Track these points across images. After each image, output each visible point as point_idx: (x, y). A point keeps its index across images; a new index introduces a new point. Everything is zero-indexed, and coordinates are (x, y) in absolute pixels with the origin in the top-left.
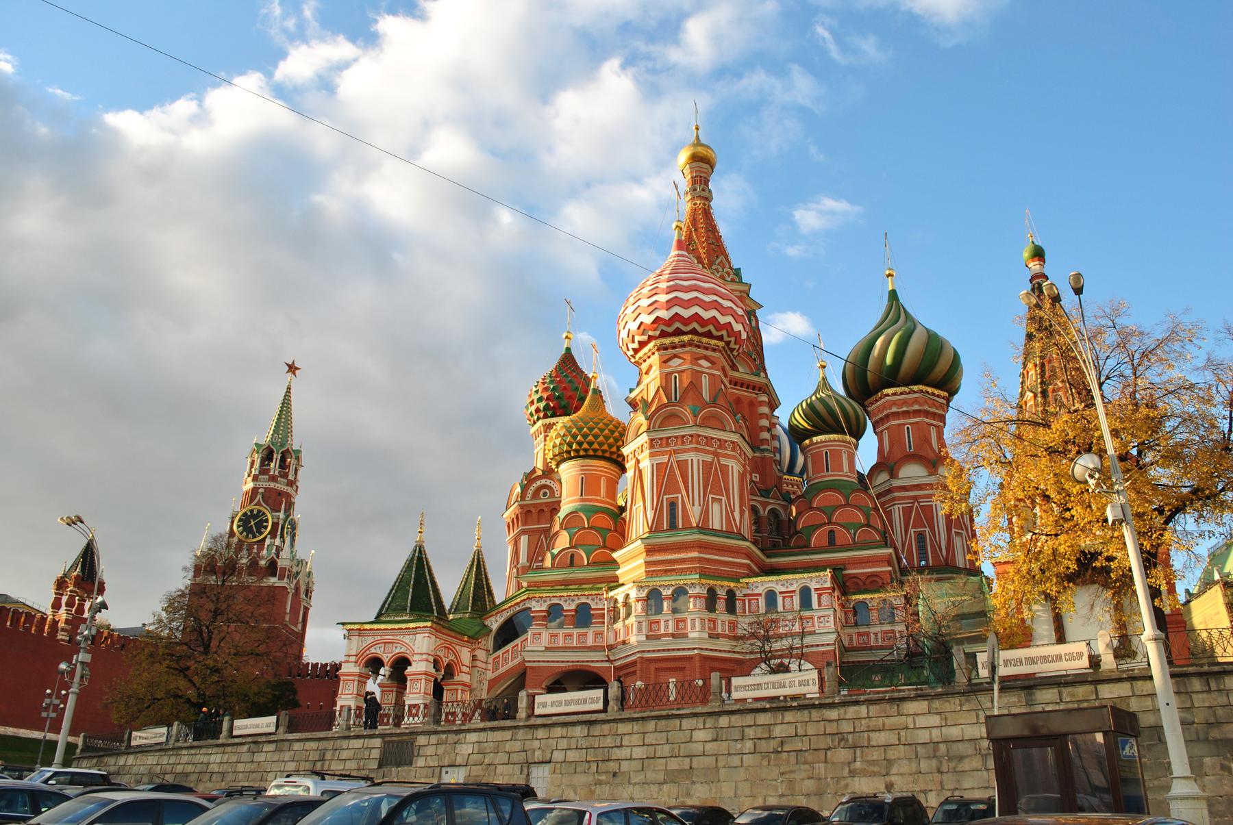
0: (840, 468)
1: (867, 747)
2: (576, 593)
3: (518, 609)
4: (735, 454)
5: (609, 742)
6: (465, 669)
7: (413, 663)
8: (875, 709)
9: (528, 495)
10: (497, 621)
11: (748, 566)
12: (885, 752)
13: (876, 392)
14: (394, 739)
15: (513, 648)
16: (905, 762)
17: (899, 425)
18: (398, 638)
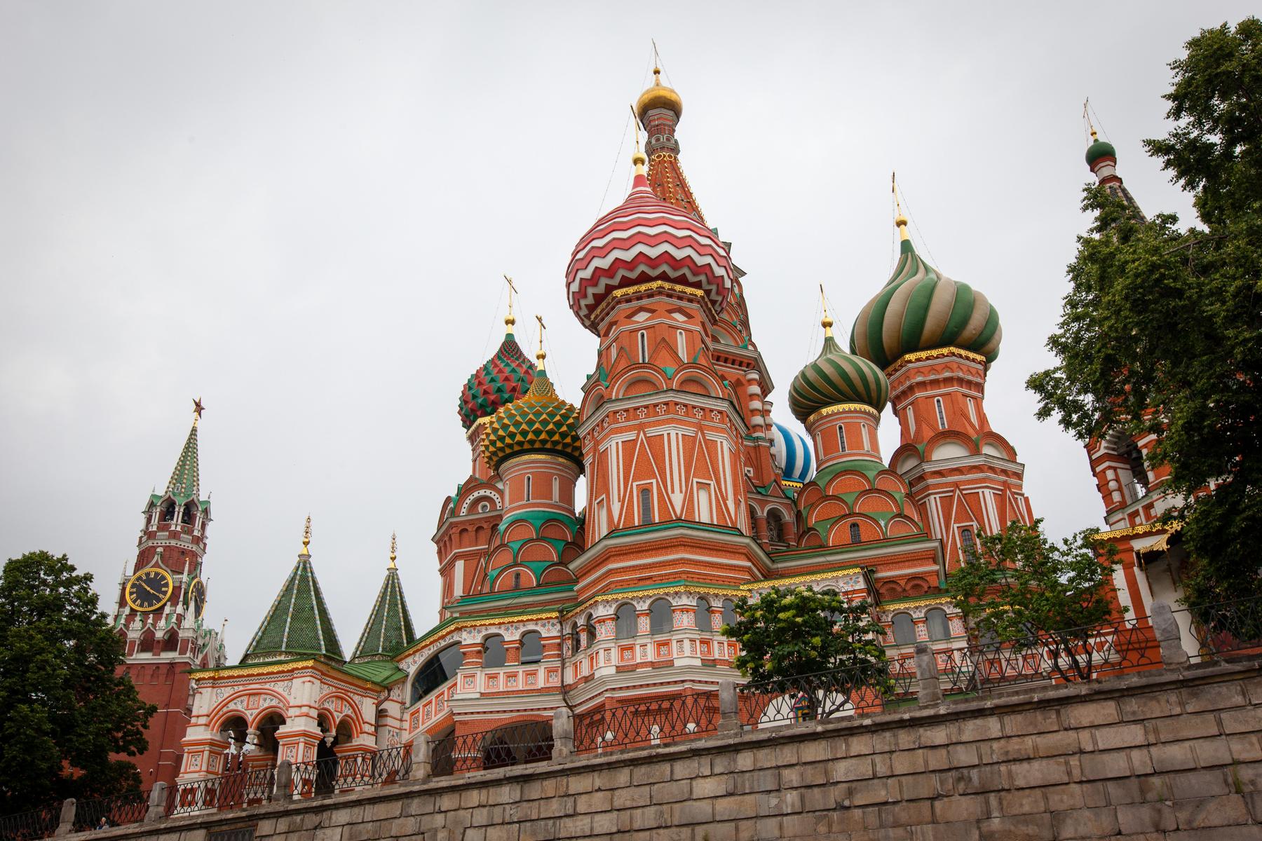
0: (861, 446)
1: (1008, 790)
2: (520, 618)
3: (443, 643)
4: (724, 426)
5: (555, 808)
6: (367, 728)
7: (288, 721)
8: (1014, 723)
9: (463, 510)
10: (415, 662)
11: (749, 570)
12: (1046, 798)
13: (895, 359)
14: (224, 828)
15: (437, 697)
16: (1087, 813)
17: (927, 398)
18: (267, 686)
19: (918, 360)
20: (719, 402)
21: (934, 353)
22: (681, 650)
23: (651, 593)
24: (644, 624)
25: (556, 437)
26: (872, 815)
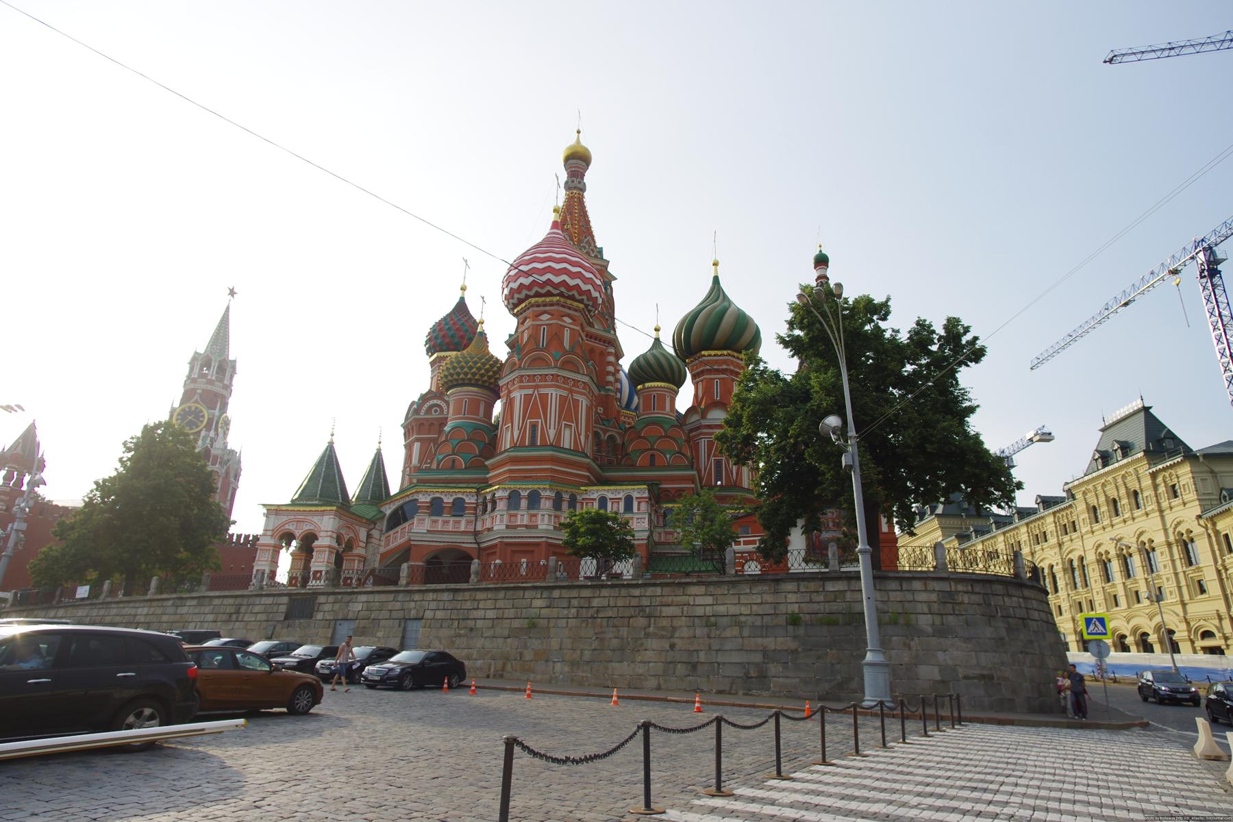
5: (468, 605)
6: (361, 544)
7: (320, 539)
8: (667, 590)
11: (588, 478)
12: (672, 621)
13: (696, 353)
16: (685, 629)
19: (709, 355)
20: (584, 377)
21: (719, 353)
22: (543, 520)
23: (530, 486)
24: (524, 503)
25: (485, 378)
26: (605, 622)
